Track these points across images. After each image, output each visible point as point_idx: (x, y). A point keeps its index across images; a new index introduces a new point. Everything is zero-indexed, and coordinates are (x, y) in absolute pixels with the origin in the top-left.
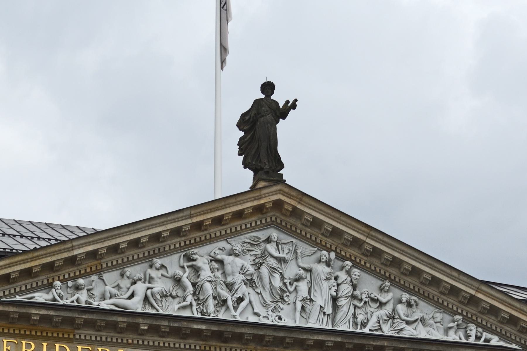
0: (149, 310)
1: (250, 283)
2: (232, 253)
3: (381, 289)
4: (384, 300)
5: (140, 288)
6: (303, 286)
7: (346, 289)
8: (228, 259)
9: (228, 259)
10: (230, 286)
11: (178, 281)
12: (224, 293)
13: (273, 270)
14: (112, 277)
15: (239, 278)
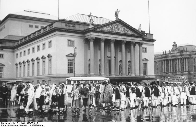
0: (109, 31)
1: (117, 28)
2: (115, 25)
3: (127, 29)
4: (127, 30)
5: (108, 29)
6: (121, 29)
7: (124, 29)
8: (115, 26)
9: (115, 26)
10: (115, 28)
11: (111, 28)
12: (115, 29)
13: (119, 27)
14: (106, 27)
15: (116, 28)
